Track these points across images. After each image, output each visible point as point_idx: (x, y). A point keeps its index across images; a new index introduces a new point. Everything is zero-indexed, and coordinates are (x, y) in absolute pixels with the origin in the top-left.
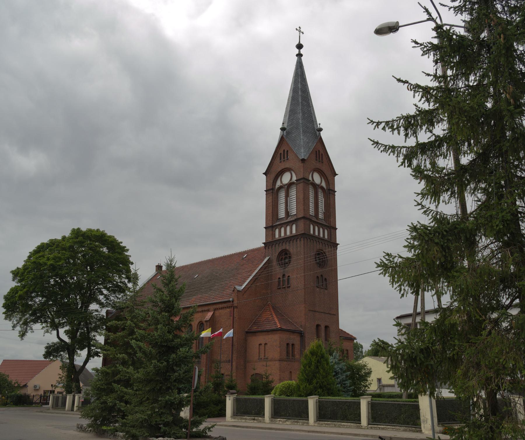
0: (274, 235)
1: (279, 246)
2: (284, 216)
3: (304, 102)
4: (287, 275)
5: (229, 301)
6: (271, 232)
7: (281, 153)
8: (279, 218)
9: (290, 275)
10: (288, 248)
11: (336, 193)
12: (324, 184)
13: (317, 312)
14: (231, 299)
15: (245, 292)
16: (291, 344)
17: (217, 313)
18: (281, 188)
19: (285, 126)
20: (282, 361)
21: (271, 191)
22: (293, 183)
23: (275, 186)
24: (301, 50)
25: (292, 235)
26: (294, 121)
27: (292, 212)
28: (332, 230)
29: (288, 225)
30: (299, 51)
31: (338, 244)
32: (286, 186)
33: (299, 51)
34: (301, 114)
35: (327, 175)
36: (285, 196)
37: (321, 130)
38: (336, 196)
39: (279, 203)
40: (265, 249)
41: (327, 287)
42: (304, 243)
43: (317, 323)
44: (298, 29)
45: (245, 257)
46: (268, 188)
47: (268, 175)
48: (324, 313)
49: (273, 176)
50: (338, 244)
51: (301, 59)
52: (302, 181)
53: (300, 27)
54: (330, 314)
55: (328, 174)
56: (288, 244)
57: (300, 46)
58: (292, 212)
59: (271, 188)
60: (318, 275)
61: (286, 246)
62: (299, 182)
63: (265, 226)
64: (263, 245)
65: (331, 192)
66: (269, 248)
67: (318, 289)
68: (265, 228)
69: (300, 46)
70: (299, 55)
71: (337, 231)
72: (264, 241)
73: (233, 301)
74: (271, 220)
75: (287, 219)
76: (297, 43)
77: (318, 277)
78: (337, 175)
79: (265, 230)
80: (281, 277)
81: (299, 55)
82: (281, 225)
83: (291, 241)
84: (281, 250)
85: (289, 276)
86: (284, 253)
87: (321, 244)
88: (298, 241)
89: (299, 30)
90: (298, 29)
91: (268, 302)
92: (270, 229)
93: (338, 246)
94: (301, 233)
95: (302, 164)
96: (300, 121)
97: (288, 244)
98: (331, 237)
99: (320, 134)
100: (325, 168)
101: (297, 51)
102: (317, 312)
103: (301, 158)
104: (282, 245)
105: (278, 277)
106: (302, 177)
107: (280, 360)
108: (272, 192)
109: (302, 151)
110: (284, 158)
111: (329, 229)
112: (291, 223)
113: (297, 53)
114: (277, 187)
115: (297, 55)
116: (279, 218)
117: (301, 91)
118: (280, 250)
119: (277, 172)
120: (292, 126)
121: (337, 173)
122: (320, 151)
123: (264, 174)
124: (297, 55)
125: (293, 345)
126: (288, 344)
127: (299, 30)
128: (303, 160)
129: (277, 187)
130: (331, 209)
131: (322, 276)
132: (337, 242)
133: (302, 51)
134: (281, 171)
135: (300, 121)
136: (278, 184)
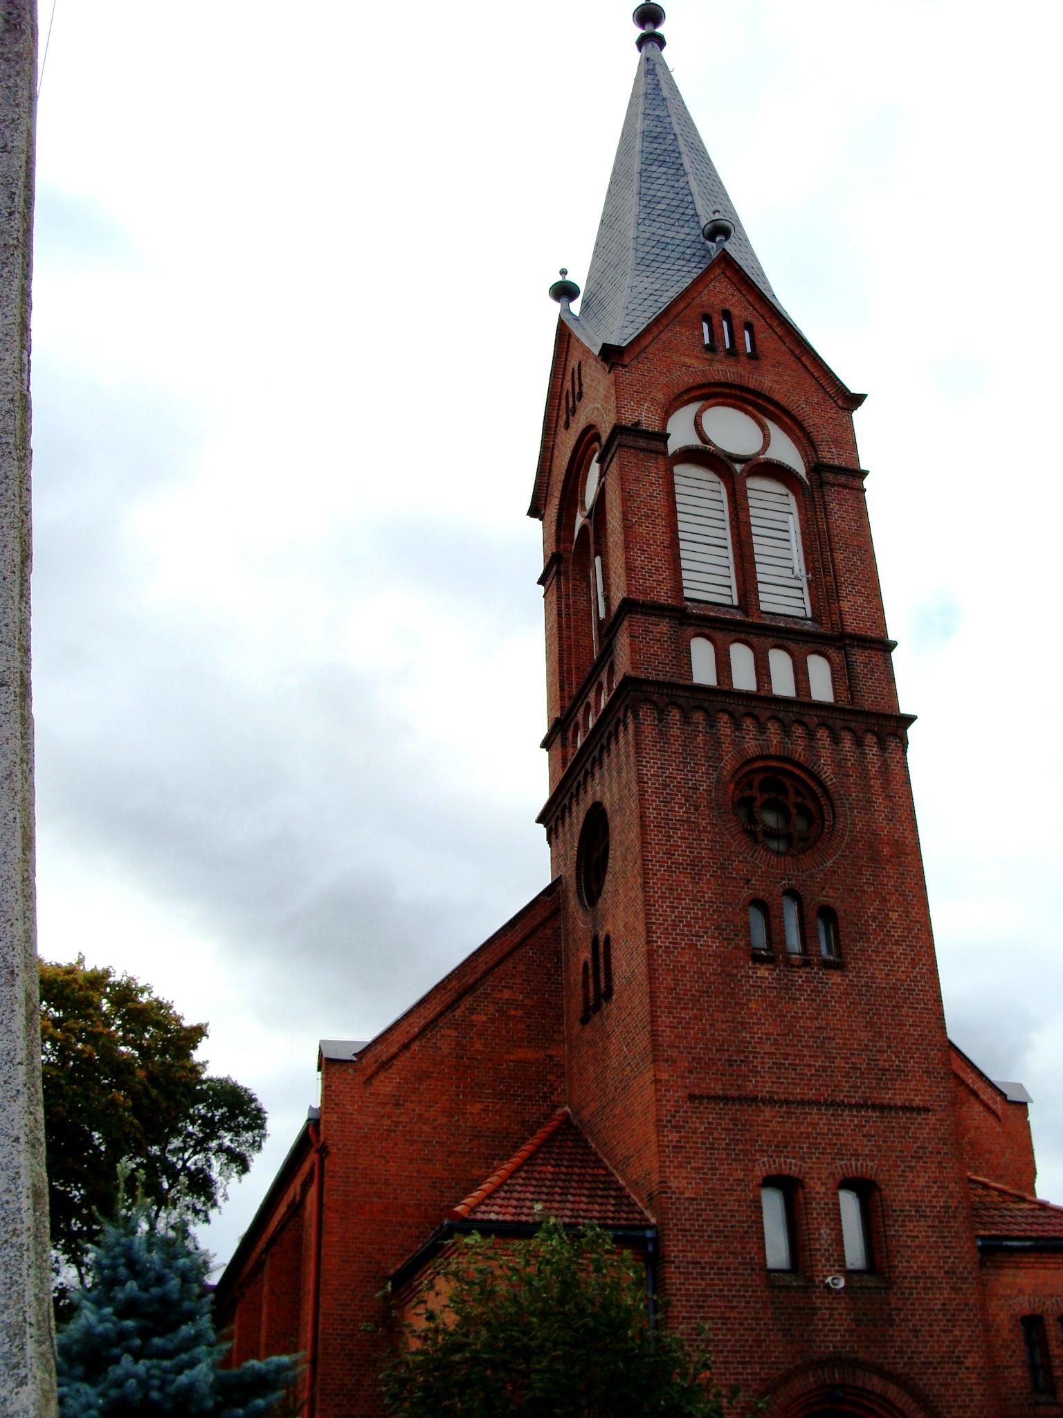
11: (867, 483)
13: (770, 1101)
15: (385, 1065)
28: (859, 656)
31: (910, 719)
35: (793, 408)
38: (868, 496)
41: (839, 955)
42: (638, 733)
48: (833, 1104)
50: (910, 719)
54: (882, 1108)
55: (802, 401)
65: (830, 477)
67: (763, 972)
71: (895, 654)
87: (772, 727)
91: (554, 1107)
93: (912, 732)
98: (851, 689)
100: (766, 380)
102: (770, 1101)
105: (582, 960)
111: (837, 657)
118: (582, 816)
121: (854, 389)
122: (735, 311)
130: (839, 556)
132: (904, 709)
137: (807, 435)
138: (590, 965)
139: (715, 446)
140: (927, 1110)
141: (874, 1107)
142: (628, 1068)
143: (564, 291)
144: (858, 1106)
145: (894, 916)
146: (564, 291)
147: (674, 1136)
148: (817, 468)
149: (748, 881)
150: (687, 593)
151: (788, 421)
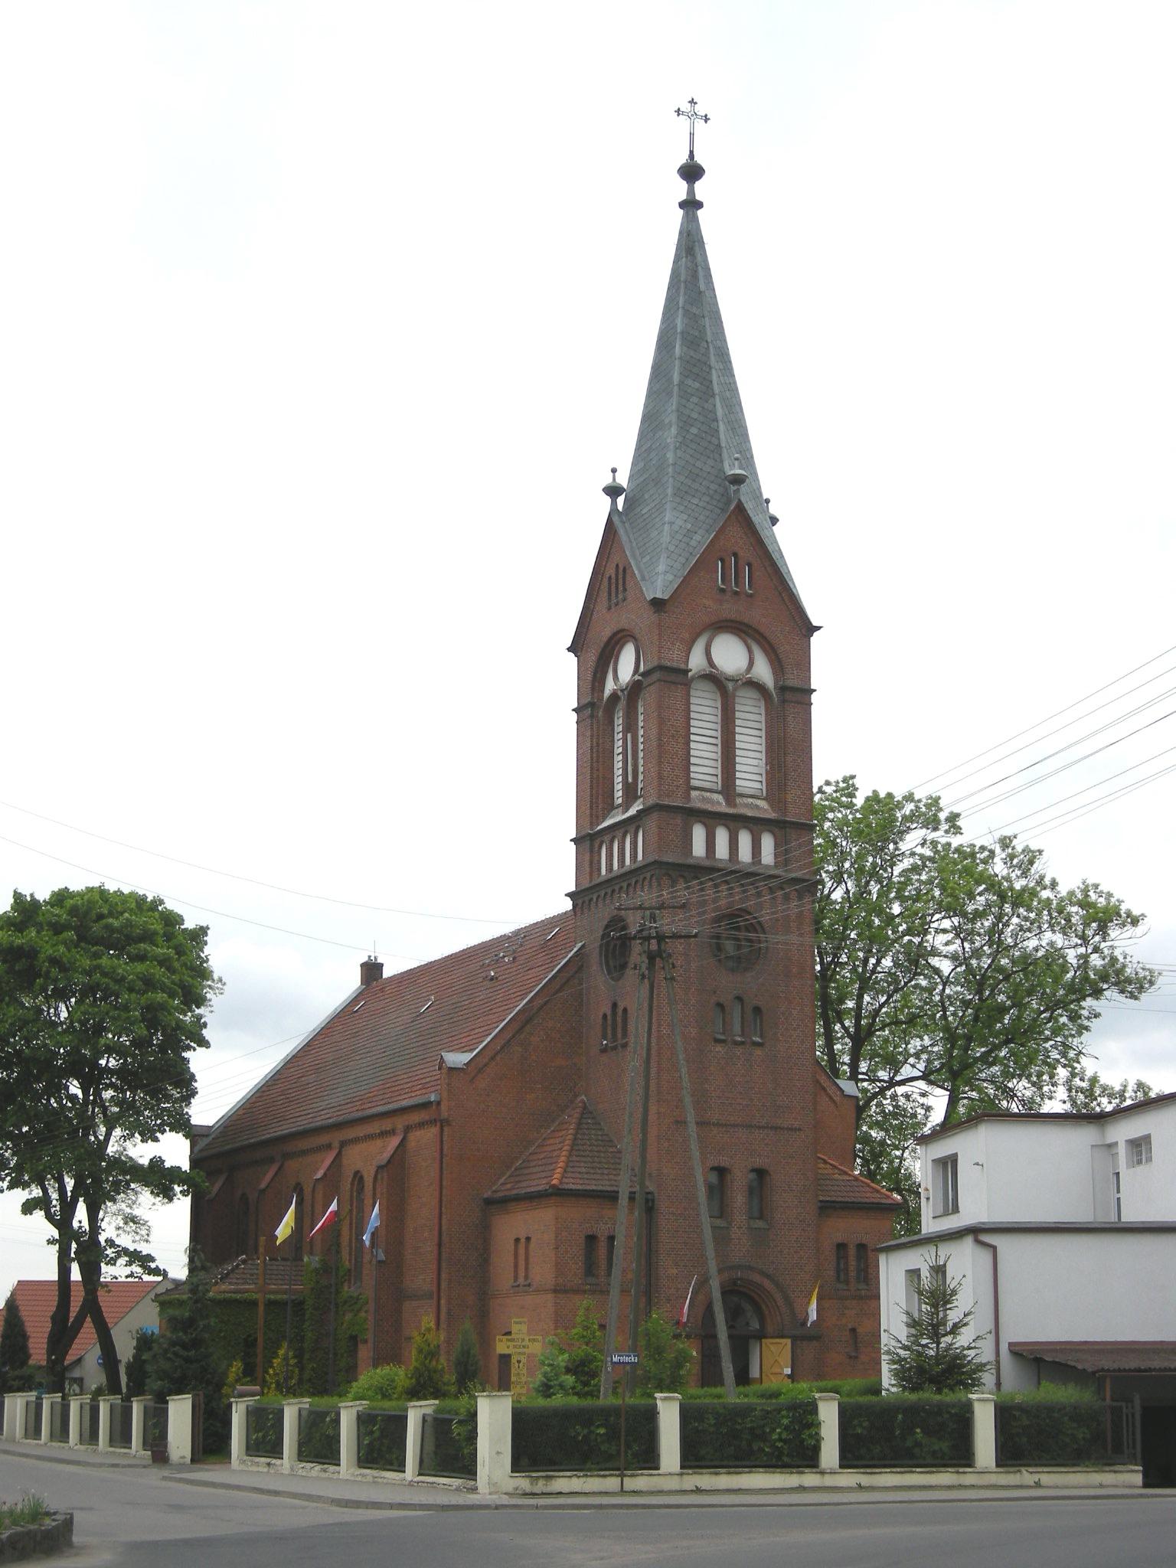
0: (595, 865)
3: (689, 382)
4: (621, 1007)
5: (426, 1105)
7: (610, 578)
11: (814, 697)
12: (763, 671)
13: (718, 1125)
15: (480, 1071)
18: (614, 696)
19: (623, 480)
20: (566, 1292)
23: (603, 691)
24: (698, 185)
26: (653, 455)
30: (691, 191)
33: (691, 191)
34: (674, 430)
38: (814, 708)
40: (575, 912)
44: (686, 107)
48: (751, 1126)
49: (592, 657)
51: (695, 220)
52: (656, 676)
53: (692, 102)
54: (776, 1128)
57: (691, 172)
60: (721, 1001)
64: (567, 905)
67: (719, 1048)
69: (691, 172)
70: (691, 205)
74: (588, 812)
75: (627, 810)
76: (683, 159)
78: (818, 628)
80: (609, 1013)
81: (691, 205)
83: (631, 890)
89: (692, 113)
90: (686, 107)
91: (576, 1096)
95: (654, 617)
96: (670, 456)
100: (755, 616)
101: (681, 189)
102: (718, 1125)
103: (649, 596)
106: (656, 663)
107: (555, 1291)
109: (661, 568)
110: (617, 596)
113: (683, 196)
114: (607, 692)
115: (682, 205)
117: (683, 339)
119: (602, 645)
121: (815, 623)
122: (741, 554)
124: (682, 205)
125: (611, 1239)
127: (692, 113)
128: (657, 604)
129: (607, 692)
133: (701, 189)
135: (670, 456)
137: (780, 661)
138: (609, 1017)
139: (717, 670)
140: (800, 1130)
141: (771, 1128)
143: (613, 491)
144: (763, 1128)
145: (795, 1012)
146: (613, 491)
147: (666, 1144)
148: (783, 689)
149: (715, 992)
150: (694, 783)
151: (767, 646)
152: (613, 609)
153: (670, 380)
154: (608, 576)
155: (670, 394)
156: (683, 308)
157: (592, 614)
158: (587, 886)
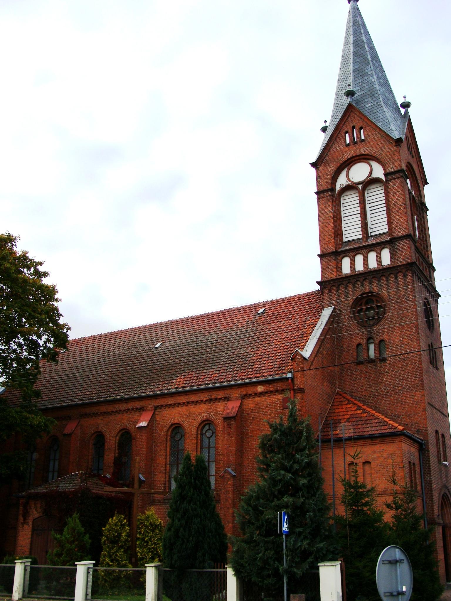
0: (339, 268)
1: (354, 287)
2: (361, 236)
5: (287, 379)
6: (333, 264)
8: (344, 240)
9: (385, 337)
10: (376, 289)
14: (289, 375)
16: (412, 463)
17: (250, 403)
21: (330, 193)
22: (377, 181)
25: (382, 268)
27: (374, 230)
29: (384, 248)
32: (360, 187)
36: (360, 203)
37: (406, 105)
39: (343, 216)
43: (435, 429)
45: (263, 313)
46: (322, 189)
47: (321, 168)
49: (331, 168)
52: (399, 175)
56: (375, 283)
58: (374, 230)
59: (330, 187)
61: (375, 287)
62: (390, 177)
63: (319, 253)
64: (318, 287)
66: (330, 291)
68: (320, 256)
72: (320, 279)
73: (292, 379)
74: (333, 241)
77: (429, 345)
79: (319, 259)
82: (357, 250)
83: (384, 279)
84: (360, 293)
85: (382, 341)
86: (364, 301)
88: (400, 278)
91: (336, 388)
92: (331, 257)
94: (403, 263)
97: (375, 283)
99: (407, 112)
104: (362, 285)
105: (356, 342)
106: (398, 168)
108: (332, 195)
112: (378, 247)
114: (338, 187)
116: (344, 240)
119: (341, 162)
120: (362, 93)
123: (313, 165)
126: (410, 462)
129: (338, 187)
131: (431, 343)
134: (348, 159)
136: (342, 181)
142: (401, 388)
152: (351, 146)
153: (366, 59)
154: (344, 131)
155: (368, 64)
156: (361, 34)
157: (330, 149)
158: (335, 278)
